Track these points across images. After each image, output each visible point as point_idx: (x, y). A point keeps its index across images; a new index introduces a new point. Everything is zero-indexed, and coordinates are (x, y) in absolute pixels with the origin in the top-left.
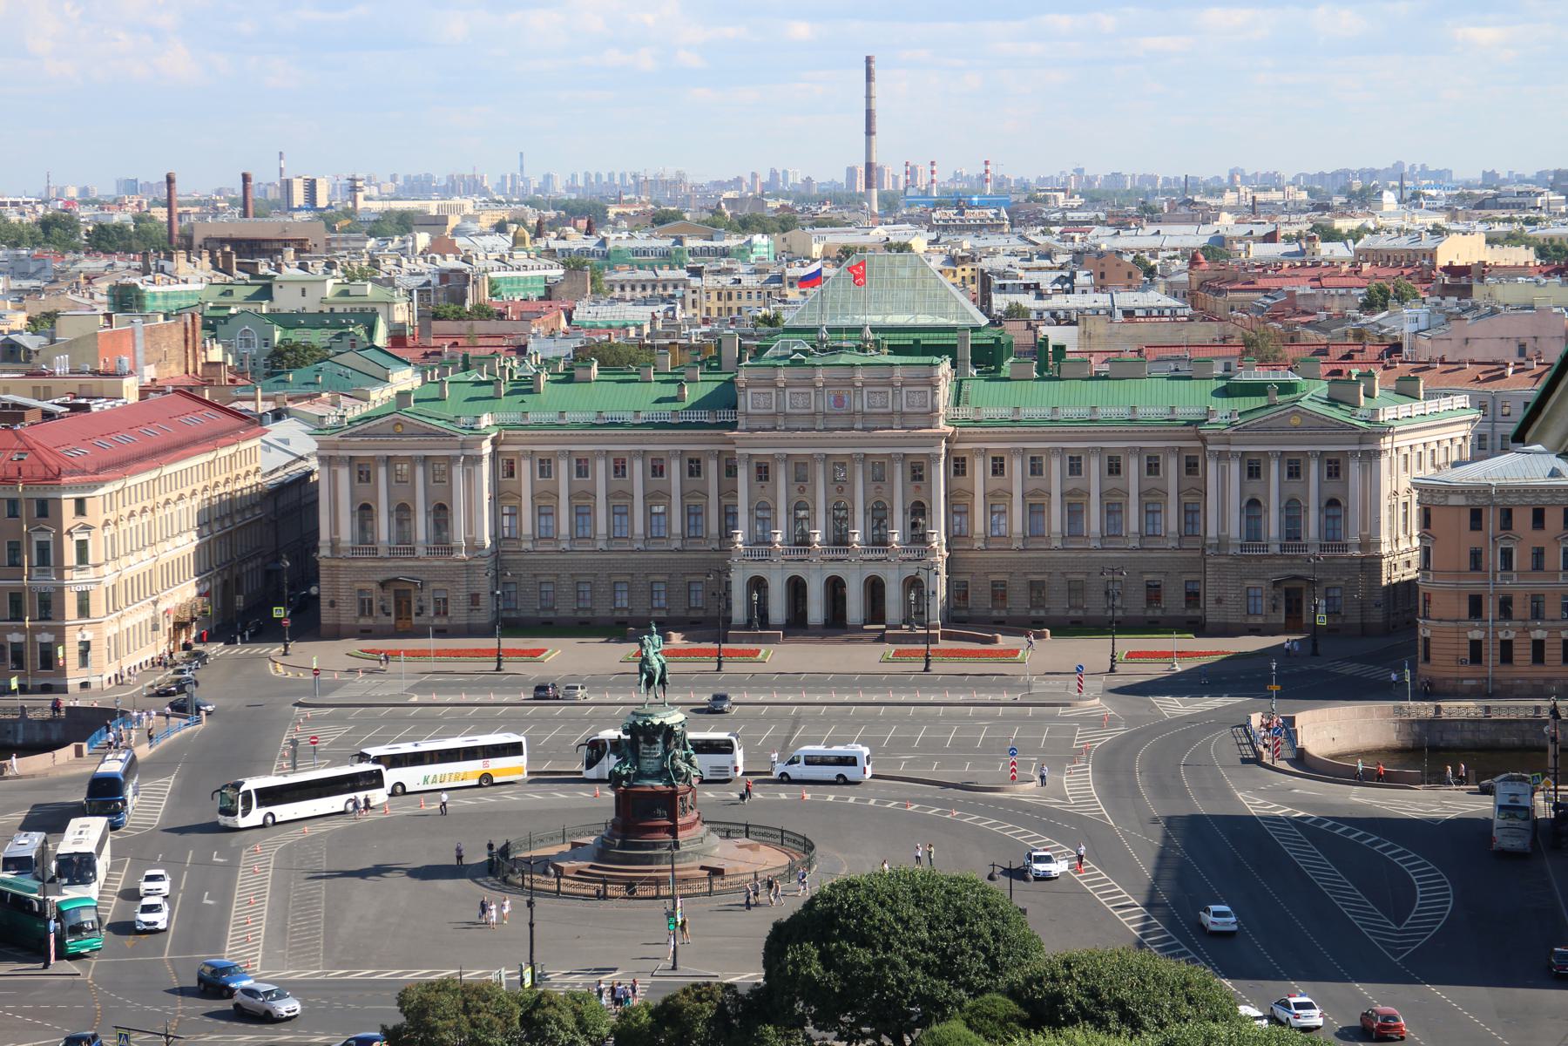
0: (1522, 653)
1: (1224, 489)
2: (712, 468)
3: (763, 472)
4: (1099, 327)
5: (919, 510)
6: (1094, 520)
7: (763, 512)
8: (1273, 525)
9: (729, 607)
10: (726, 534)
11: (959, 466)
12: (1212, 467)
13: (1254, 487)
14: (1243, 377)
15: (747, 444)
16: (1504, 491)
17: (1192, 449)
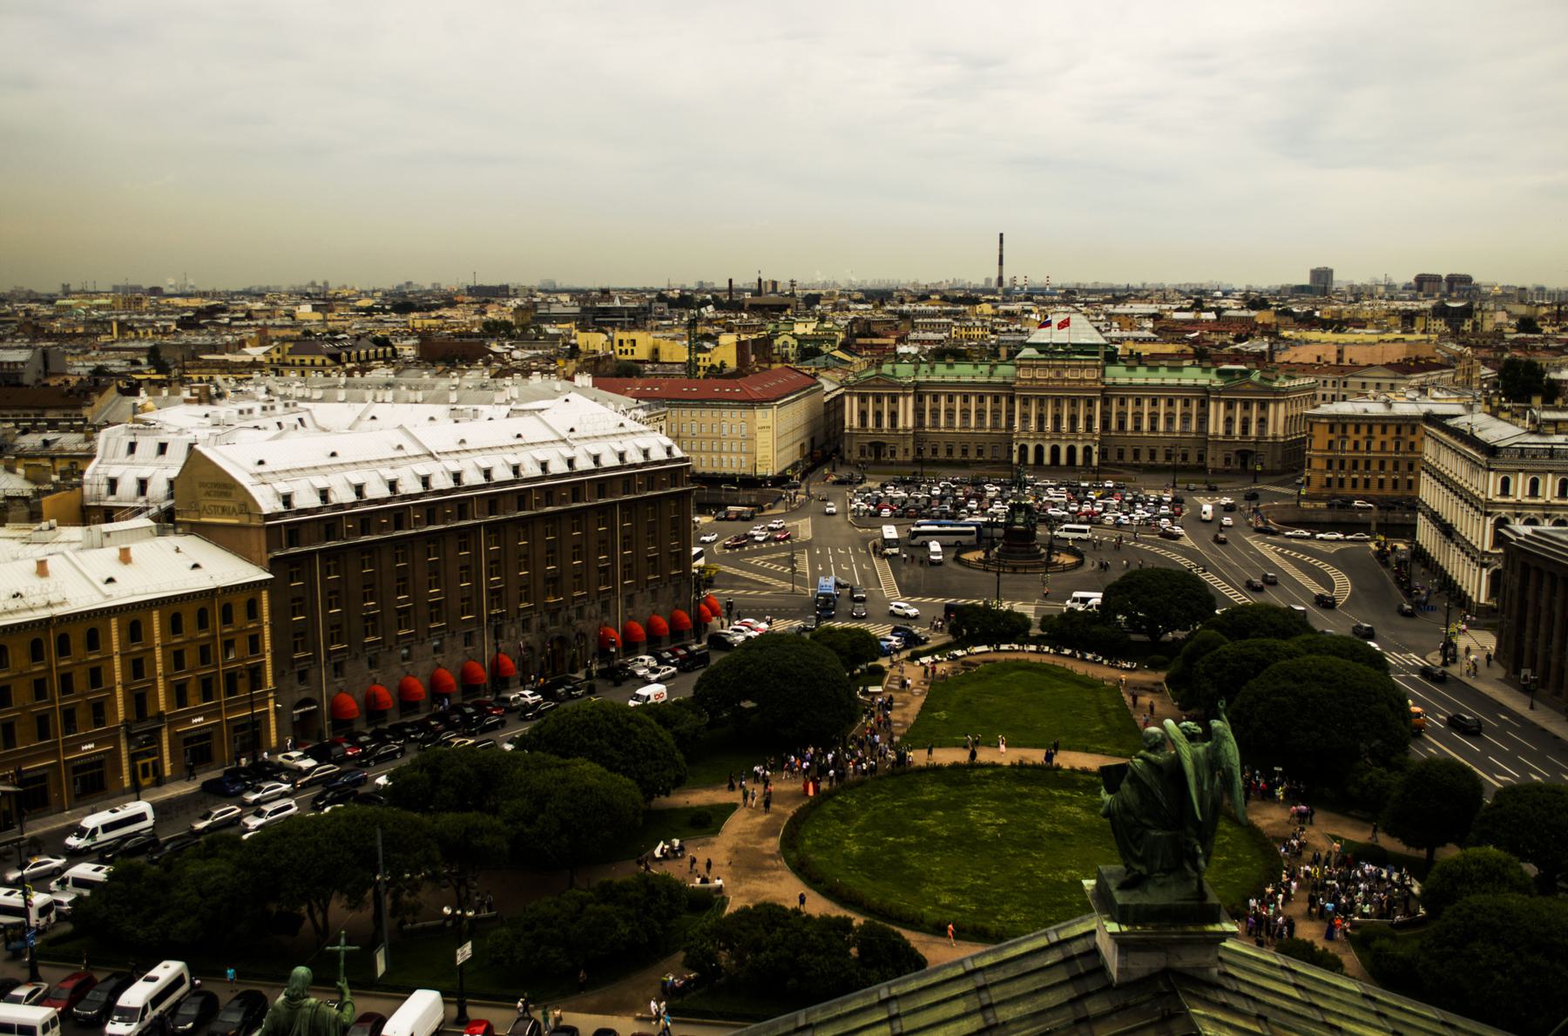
0: (1348, 484)
4: (1130, 345)
5: (1089, 419)
7: (1025, 417)
8: (1237, 430)
10: (1010, 426)
11: (1106, 401)
12: (1212, 405)
13: (1230, 413)
14: (1226, 367)
16: (1344, 417)
17: (1205, 395)
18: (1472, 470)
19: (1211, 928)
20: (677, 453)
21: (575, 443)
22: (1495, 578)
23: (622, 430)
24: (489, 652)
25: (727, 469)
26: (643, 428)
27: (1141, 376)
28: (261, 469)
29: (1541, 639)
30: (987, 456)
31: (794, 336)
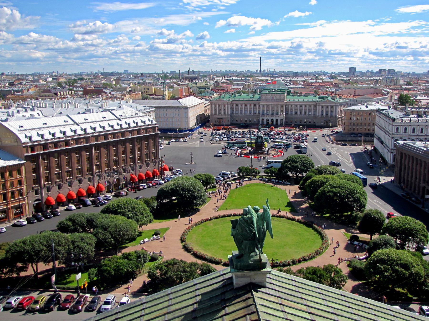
1: (319, 109)
2: (257, 106)
3: (263, 106)
5: (282, 111)
6: (303, 113)
8: (324, 114)
9: (259, 122)
10: (259, 113)
12: (317, 107)
13: (323, 109)
15: (262, 103)
17: (315, 104)
18: (388, 125)
19: (264, 270)
20: (154, 122)
21: (122, 120)
22: (395, 155)
23: (137, 115)
24: (96, 184)
25: (174, 127)
26: (144, 115)
27: (296, 98)
28: (21, 129)
29: (406, 174)
30: (252, 122)
31: (197, 87)
